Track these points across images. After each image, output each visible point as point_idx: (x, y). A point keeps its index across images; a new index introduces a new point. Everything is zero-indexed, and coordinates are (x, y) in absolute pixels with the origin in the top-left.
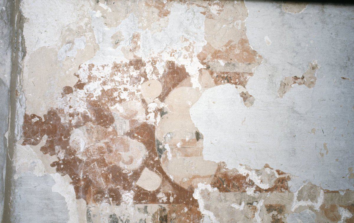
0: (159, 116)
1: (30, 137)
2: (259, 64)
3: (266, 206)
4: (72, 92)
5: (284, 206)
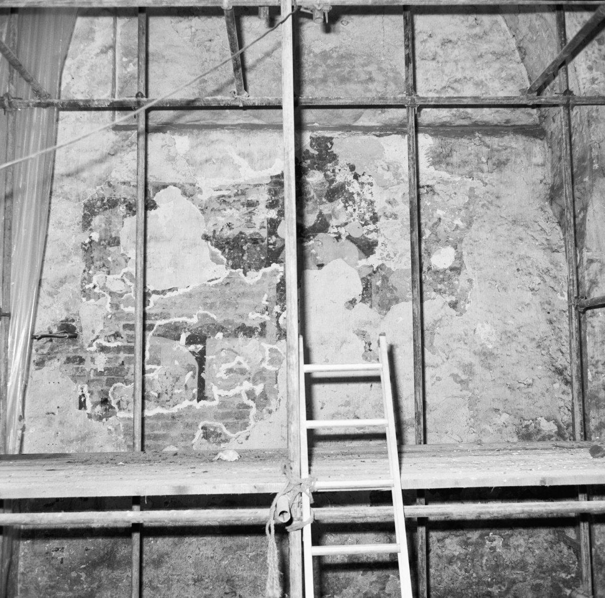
0: (335, 235)
1: (316, 141)
2: (380, 313)
3: (265, 322)
4: (351, 171)
5: (265, 337)
